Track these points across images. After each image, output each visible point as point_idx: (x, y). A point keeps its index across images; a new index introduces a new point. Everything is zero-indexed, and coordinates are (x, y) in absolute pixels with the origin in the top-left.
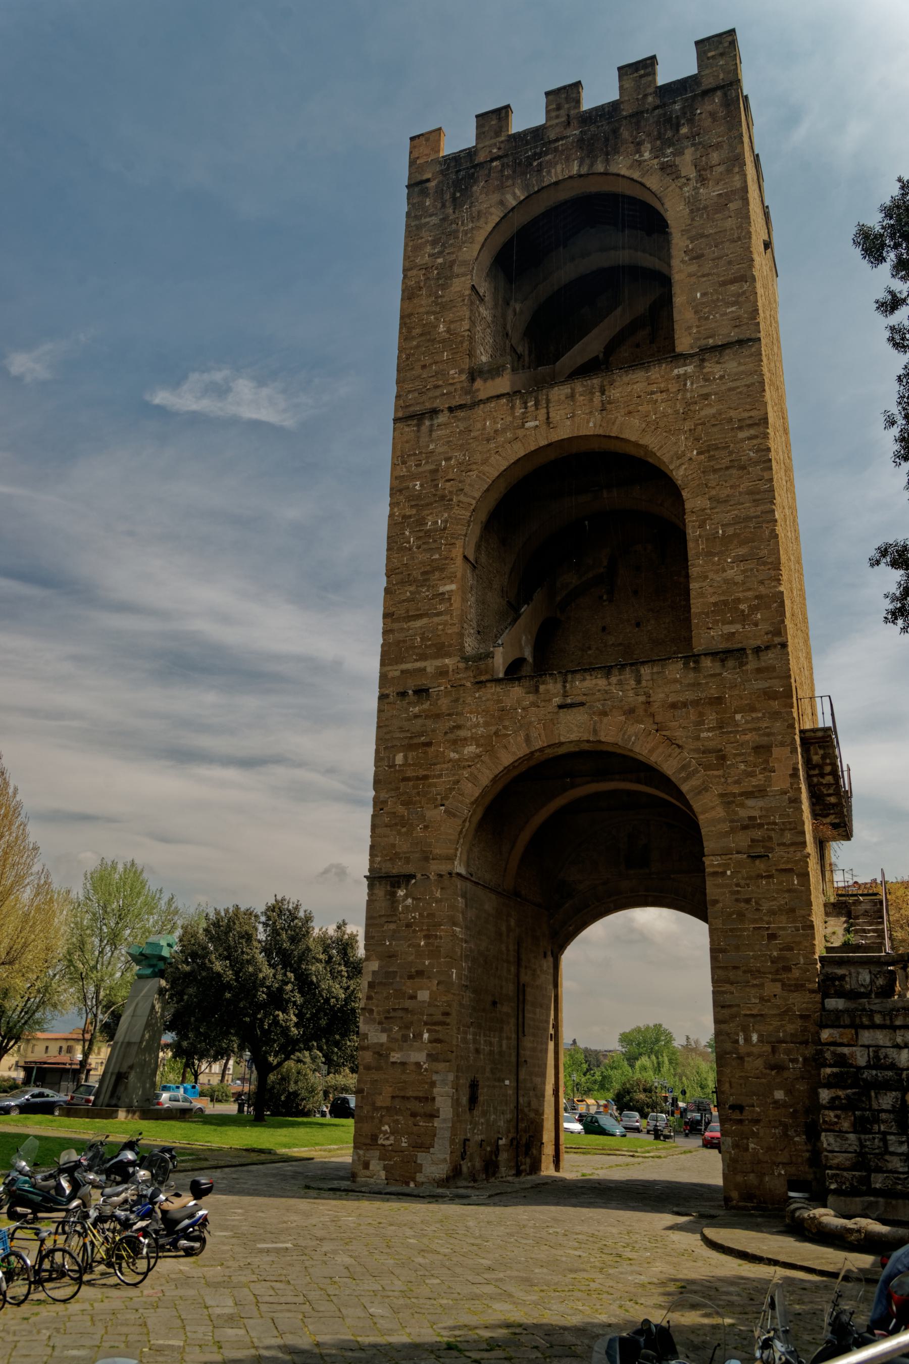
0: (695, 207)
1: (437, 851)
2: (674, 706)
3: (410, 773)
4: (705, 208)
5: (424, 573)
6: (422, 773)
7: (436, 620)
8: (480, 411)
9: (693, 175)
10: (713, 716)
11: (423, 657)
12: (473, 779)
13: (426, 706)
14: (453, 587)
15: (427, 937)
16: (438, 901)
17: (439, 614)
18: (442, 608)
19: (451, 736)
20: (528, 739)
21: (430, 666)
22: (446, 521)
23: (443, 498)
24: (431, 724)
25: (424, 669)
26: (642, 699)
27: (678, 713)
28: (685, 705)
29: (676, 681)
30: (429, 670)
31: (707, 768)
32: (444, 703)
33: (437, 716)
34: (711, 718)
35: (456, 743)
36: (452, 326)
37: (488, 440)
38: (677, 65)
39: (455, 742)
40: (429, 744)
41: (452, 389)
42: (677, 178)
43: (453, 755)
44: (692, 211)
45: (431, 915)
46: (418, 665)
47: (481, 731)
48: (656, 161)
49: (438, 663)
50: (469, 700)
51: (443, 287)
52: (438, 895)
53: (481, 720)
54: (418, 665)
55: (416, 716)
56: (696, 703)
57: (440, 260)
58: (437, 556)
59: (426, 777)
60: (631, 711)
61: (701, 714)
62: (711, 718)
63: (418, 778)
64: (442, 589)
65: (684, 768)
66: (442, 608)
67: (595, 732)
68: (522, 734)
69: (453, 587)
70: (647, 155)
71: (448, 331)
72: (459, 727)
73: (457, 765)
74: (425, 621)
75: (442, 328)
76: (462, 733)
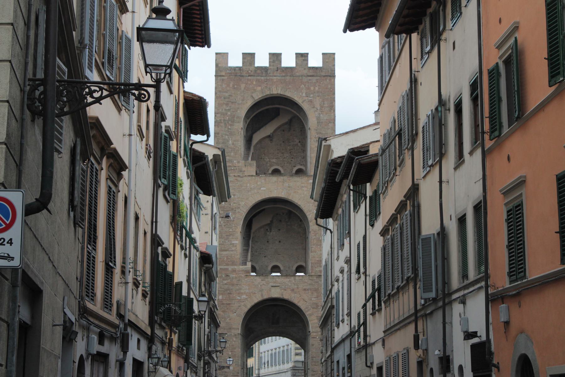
0: (319, 122)
1: (234, 327)
2: (305, 290)
3: (224, 302)
4: (322, 123)
5: (227, 236)
6: (228, 302)
7: (232, 252)
8: (245, 178)
9: (319, 108)
10: (316, 294)
11: (227, 265)
12: (245, 306)
13: (229, 281)
14: (237, 242)
15: (231, 352)
16: (235, 341)
17: (232, 251)
18: (233, 249)
19: (238, 292)
20: (262, 295)
21: (230, 268)
22: (234, 218)
23: (232, 209)
24: (231, 287)
25: (227, 269)
26: (296, 286)
27: (307, 292)
28: (308, 290)
29: (306, 282)
30: (230, 269)
31: (313, 308)
32: (235, 281)
33: (233, 285)
34: (315, 294)
35: (240, 294)
36: (235, 143)
37: (248, 191)
38: (315, 61)
39: (239, 293)
40: (231, 294)
41: (235, 168)
42: (314, 107)
43: (238, 298)
44: (318, 123)
45: (233, 345)
46: (226, 267)
47: (247, 291)
48: (306, 98)
49: (233, 267)
50: (243, 281)
51: (231, 125)
52: (235, 339)
53: (247, 288)
54: (226, 267)
55: (226, 284)
56: (310, 289)
57: (229, 113)
58: (231, 230)
59: (229, 304)
60: (293, 290)
61: (312, 293)
62: (315, 294)
63: (227, 304)
64: (233, 242)
65: (307, 308)
66: (233, 249)
67: (282, 295)
68: (260, 293)
69: (237, 242)
70: (304, 95)
71: (233, 144)
72: (240, 289)
73: (240, 301)
74: (227, 252)
75: (230, 142)
76: (242, 291)
